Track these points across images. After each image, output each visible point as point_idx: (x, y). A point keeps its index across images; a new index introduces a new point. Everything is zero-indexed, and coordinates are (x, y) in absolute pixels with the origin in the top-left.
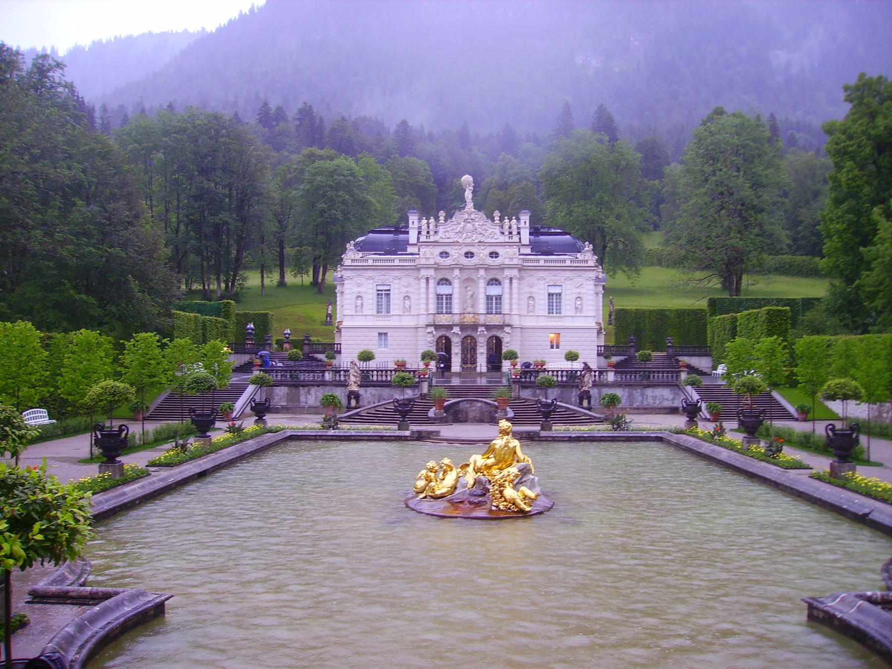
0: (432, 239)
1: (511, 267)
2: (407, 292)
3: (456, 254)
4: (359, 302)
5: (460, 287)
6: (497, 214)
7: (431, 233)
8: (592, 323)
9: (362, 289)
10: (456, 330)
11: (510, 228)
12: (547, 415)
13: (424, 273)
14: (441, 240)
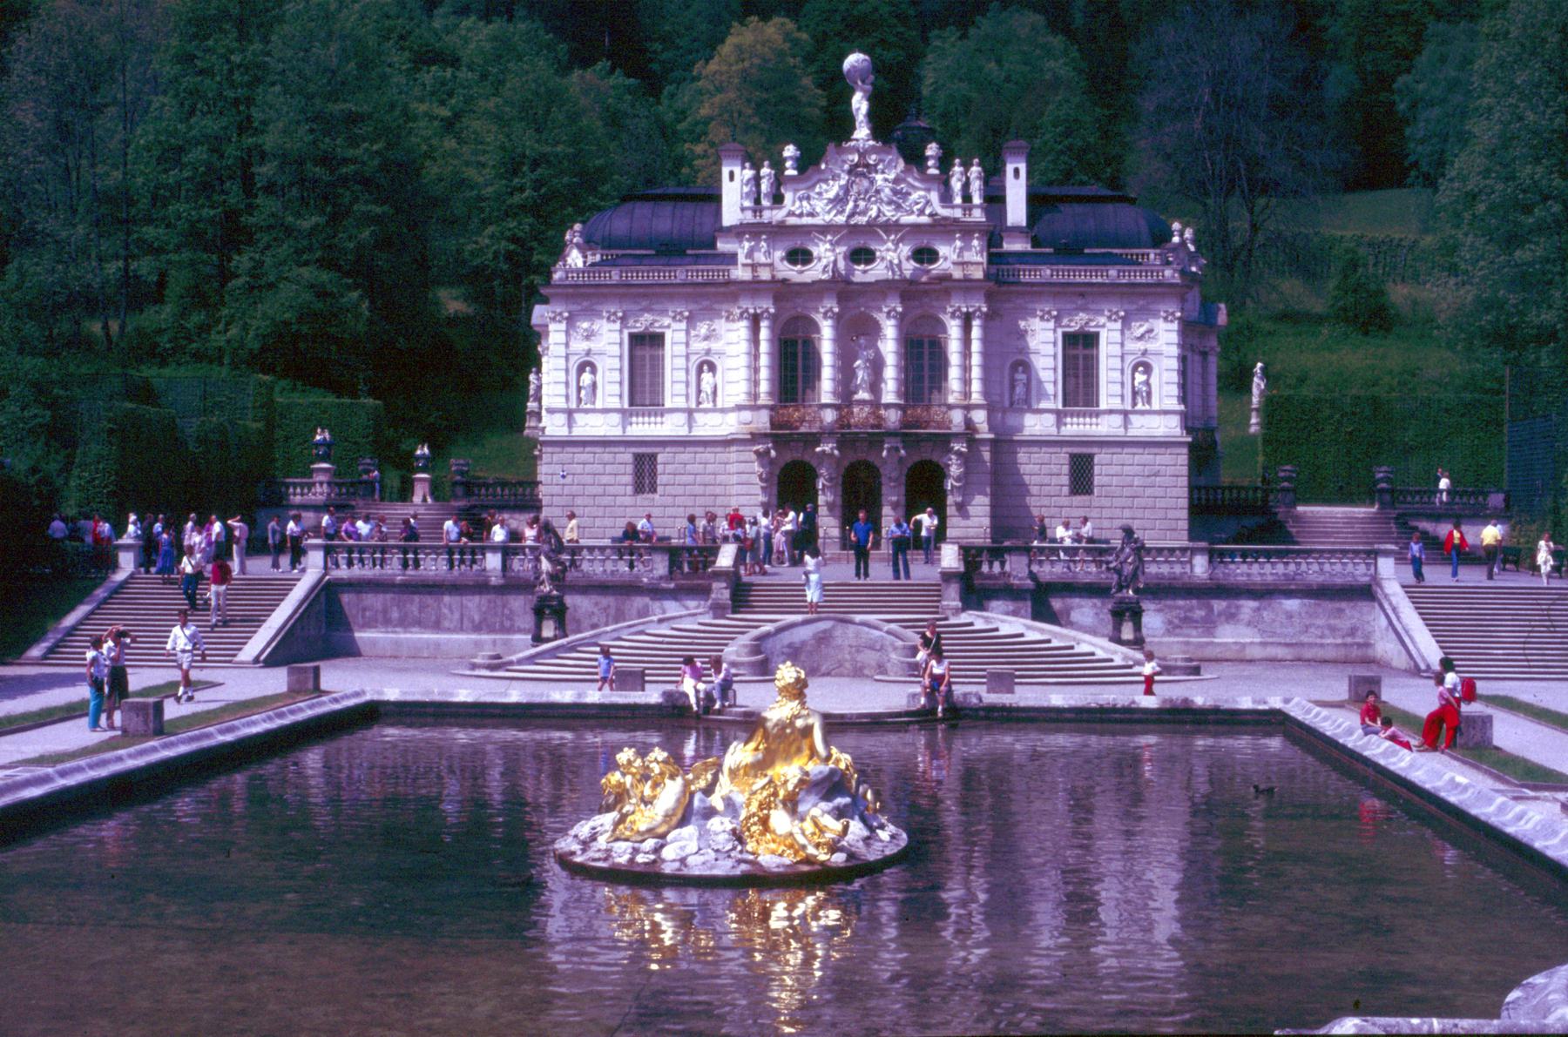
0: (767, 216)
2: (708, 352)
4: (587, 378)
5: (839, 340)
6: (932, 150)
7: (765, 203)
8: (1171, 428)
9: (593, 345)
10: (826, 447)
11: (966, 186)
14: (792, 221)
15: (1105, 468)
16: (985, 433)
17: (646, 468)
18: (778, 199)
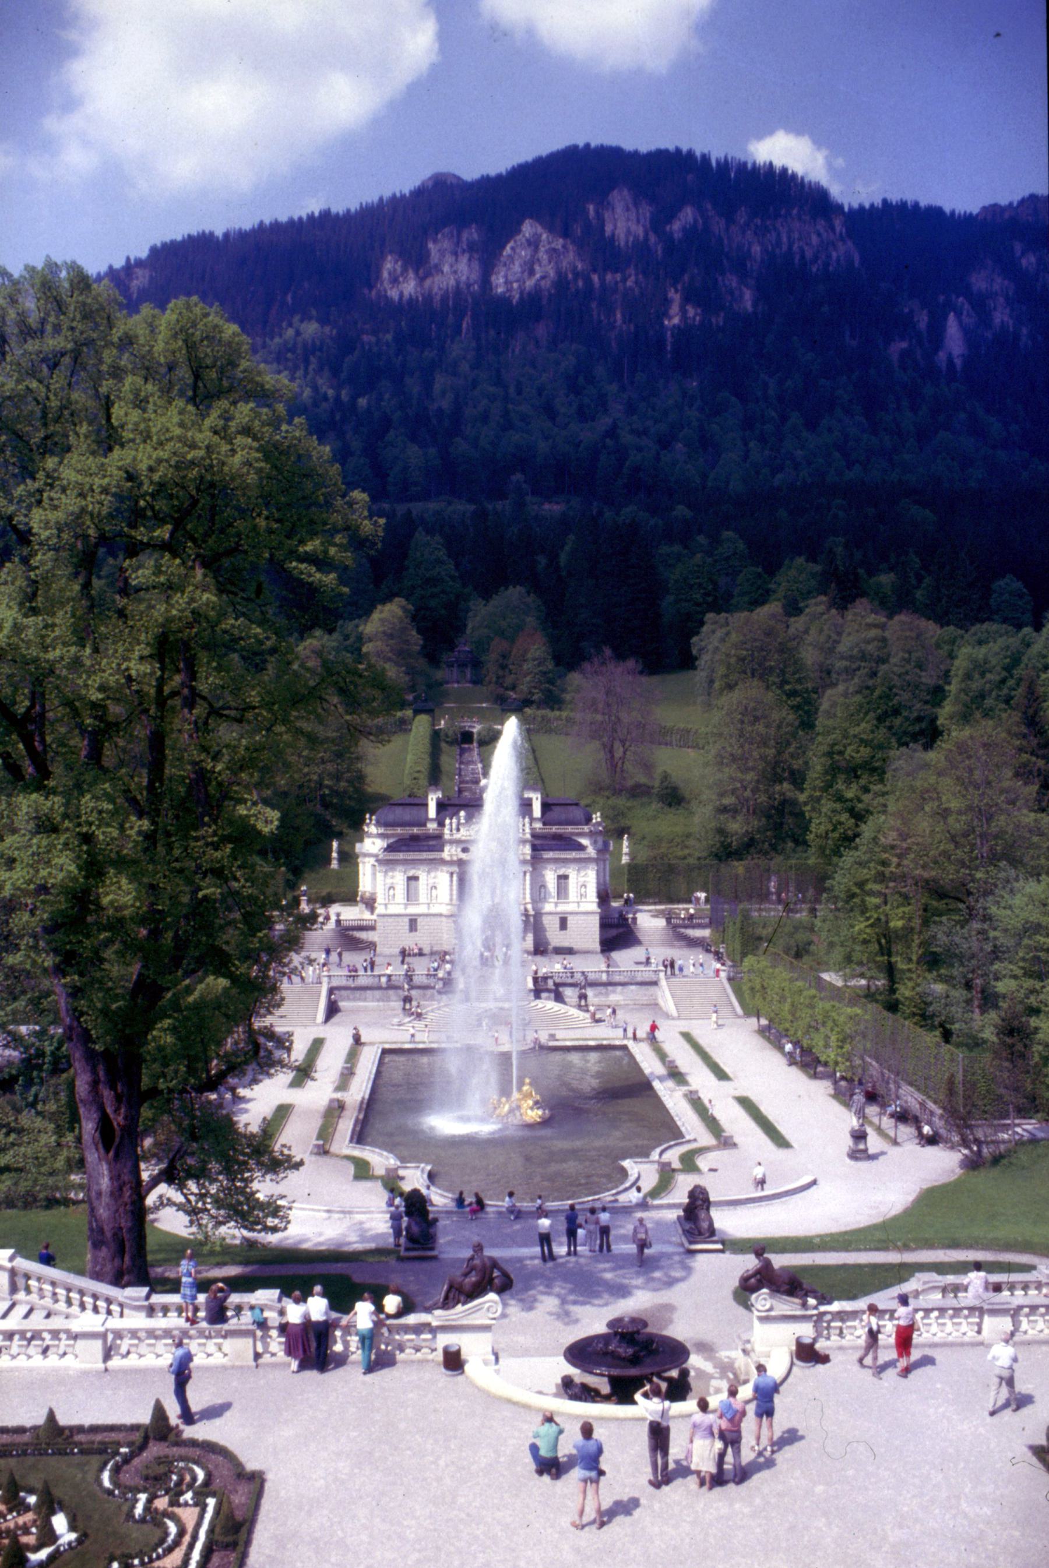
15: (571, 921)
16: (532, 912)
17: (413, 924)
18: (458, 830)
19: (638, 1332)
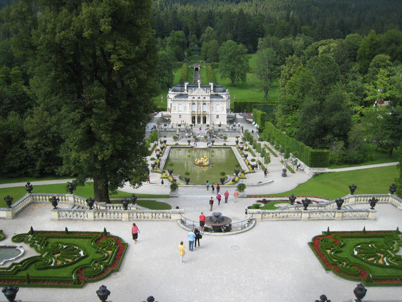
1: (208, 101)
3: (196, 98)
10: (196, 115)
12: (213, 143)
13: (189, 102)
17: (180, 116)
19: (219, 216)
